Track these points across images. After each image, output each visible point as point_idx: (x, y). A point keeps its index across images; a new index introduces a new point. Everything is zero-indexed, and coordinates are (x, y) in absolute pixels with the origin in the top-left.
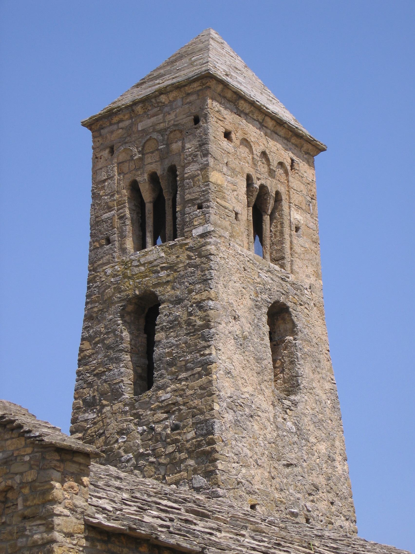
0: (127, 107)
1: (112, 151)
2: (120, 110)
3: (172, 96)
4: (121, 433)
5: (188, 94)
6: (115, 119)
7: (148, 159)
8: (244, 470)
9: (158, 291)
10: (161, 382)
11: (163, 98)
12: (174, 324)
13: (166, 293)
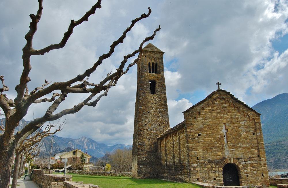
0: (150, 51)
1: (146, 56)
2: (148, 51)
4: (151, 99)
6: (147, 52)
7: (152, 60)
10: (157, 94)
11: (156, 53)
12: (159, 86)
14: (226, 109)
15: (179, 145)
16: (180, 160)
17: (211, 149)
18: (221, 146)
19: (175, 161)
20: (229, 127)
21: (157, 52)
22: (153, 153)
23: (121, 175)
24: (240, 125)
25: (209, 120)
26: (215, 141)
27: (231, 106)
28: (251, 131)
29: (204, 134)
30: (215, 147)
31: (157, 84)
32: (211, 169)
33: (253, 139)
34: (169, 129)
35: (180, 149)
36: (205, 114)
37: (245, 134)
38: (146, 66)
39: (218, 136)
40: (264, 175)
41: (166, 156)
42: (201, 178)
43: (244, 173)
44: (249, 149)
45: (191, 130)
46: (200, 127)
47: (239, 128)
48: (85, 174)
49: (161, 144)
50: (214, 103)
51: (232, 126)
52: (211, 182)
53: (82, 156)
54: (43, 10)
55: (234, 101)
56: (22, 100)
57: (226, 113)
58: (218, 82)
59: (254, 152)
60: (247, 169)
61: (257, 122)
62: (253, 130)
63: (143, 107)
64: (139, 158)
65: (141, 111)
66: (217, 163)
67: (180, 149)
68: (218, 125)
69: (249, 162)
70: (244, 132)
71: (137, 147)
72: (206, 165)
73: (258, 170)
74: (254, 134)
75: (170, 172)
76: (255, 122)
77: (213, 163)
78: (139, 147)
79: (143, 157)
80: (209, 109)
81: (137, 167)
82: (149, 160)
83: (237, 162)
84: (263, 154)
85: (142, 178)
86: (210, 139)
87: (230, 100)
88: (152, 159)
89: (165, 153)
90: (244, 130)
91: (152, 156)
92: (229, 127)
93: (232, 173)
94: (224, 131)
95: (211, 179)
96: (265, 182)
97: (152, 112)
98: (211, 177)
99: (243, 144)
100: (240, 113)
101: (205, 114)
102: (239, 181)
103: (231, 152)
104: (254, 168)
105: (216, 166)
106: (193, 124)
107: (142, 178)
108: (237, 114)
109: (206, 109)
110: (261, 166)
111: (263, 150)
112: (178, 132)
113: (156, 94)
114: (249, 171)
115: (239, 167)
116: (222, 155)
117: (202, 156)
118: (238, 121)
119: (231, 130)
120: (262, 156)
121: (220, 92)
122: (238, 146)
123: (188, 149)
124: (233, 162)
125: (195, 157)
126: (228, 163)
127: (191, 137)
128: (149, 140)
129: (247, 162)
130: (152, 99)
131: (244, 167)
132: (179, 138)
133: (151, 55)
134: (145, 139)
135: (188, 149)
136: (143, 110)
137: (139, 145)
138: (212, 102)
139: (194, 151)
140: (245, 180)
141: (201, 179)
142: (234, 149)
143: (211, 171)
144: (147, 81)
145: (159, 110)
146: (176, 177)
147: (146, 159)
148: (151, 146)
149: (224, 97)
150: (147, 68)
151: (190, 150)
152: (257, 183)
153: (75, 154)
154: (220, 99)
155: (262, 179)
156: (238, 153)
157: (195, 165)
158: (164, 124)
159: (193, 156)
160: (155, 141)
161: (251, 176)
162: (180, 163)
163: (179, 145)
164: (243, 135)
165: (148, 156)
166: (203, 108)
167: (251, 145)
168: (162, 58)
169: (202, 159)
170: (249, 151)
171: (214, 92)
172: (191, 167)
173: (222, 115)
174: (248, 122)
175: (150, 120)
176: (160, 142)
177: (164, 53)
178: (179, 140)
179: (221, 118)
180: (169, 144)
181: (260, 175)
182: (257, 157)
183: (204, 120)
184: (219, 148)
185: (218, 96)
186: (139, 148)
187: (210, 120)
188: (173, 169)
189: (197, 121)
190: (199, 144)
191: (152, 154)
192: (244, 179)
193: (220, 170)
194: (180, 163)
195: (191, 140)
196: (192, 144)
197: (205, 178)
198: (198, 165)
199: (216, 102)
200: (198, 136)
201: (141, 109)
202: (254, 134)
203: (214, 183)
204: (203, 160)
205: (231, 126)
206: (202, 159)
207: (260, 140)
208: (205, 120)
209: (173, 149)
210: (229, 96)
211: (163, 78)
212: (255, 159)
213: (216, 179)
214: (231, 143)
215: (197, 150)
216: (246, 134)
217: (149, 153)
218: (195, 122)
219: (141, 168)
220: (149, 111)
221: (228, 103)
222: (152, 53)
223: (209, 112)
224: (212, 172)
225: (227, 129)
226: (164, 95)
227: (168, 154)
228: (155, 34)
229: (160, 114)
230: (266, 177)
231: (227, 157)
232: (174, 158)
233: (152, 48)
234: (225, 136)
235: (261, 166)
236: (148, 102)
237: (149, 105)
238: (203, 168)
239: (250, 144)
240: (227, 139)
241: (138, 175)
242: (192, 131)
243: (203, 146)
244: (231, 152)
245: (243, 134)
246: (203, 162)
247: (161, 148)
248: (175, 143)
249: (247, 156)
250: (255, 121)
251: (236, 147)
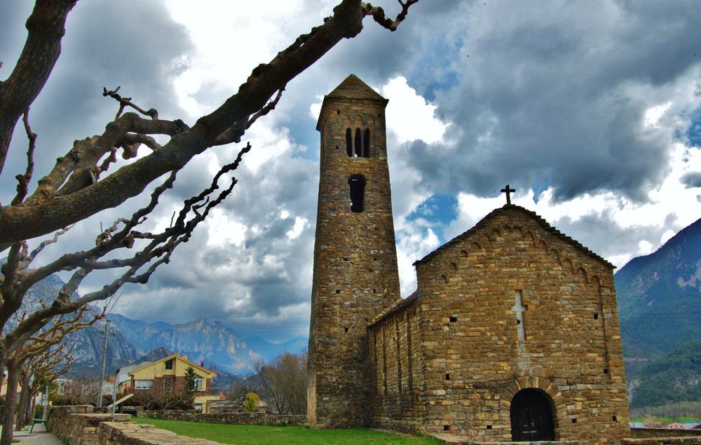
0: (349, 98)
1: (339, 113)
2: (345, 98)
3: (369, 102)
5: (376, 105)
6: (342, 101)
7: (357, 122)
9: (366, 175)
10: (369, 210)
11: (366, 102)
12: (372, 190)
14: (523, 253)
15: (409, 344)
16: (410, 381)
17: (483, 354)
18: (509, 346)
19: (402, 383)
20: (530, 299)
21: (368, 99)
22: (356, 365)
23: (287, 422)
24: (561, 294)
26: (494, 333)
27: (537, 245)
28: (587, 309)
29: (465, 316)
30: (494, 350)
31: (369, 185)
32: (480, 403)
33: (594, 328)
34: (398, 301)
35: (410, 355)
36: (470, 267)
37: (572, 316)
38: (341, 138)
39: (501, 322)
40: (618, 418)
41: (385, 372)
42: (454, 424)
44: (581, 352)
45: (433, 307)
46: (456, 299)
47: (558, 303)
48: (192, 418)
49: (375, 340)
50: (495, 240)
51: (538, 297)
52: (480, 434)
53: (190, 371)
54: (34, 167)
55: (546, 233)
56: (12, 286)
58: (507, 187)
59: (594, 360)
60: (573, 404)
61: (605, 287)
62: (596, 305)
63: (330, 247)
64: (320, 377)
65: (325, 256)
66: (495, 388)
67: (410, 355)
68: (503, 294)
69: (580, 386)
70: (571, 313)
71: (315, 349)
72: (468, 393)
73: (601, 406)
74: (596, 317)
75: (391, 412)
76: (600, 287)
77: (486, 388)
78: (320, 348)
79: (331, 375)
80: (481, 254)
81: (315, 400)
82: (346, 381)
83: (547, 387)
84: (617, 367)
85: (327, 428)
86: (482, 329)
87: (537, 232)
88: (354, 378)
89: (383, 363)
90: (570, 306)
91: (355, 371)
92: (530, 299)
93: (533, 410)
94: (517, 310)
95: (480, 427)
96: (619, 436)
97: (354, 258)
98: (480, 422)
99: (565, 342)
100: (560, 264)
101: (470, 267)
102: (553, 432)
103: (535, 360)
104: (592, 400)
105: (493, 396)
106: (438, 293)
107: (327, 428)
108: (555, 267)
109: (472, 256)
110: (612, 397)
111: (617, 356)
112: (406, 312)
113: (366, 210)
114: (579, 406)
115: (553, 398)
116: (509, 368)
117: (457, 372)
118: (554, 285)
119: (537, 306)
120: (616, 370)
122: (553, 346)
123: (424, 355)
124: (537, 387)
125: (440, 375)
126: (524, 388)
127: (431, 324)
128: (346, 330)
129: (574, 386)
130: (355, 226)
131: (567, 399)
132: (409, 327)
133: (354, 108)
134: (336, 329)
135: (424, 355)
136: (331, 254)
137: (321, 344)
138: (489, 237)
139: (439, 360)
140: (568, 431)
141: (454, 428)
142: (542, 355)
143: (480, 408)
144: (342, 177)
145: (372, 252)
146: (403, 422)
147: (337, 380)
148: (350, 345)
150: (342, 142)
151: (428, 356)
152: (600, 437)
153: (171, 368)
154: (510, 228)
155: (611, 427)
156: (551, 363)
157: (441, 392)
158: (386, 290)
159: (437, 372)
160: (363, 332)
161: (584, 419)
162: (411, 389)
163: (409, 344)
164: (566, 319)
165: (344, 372)
166: (465, 253)
167: (588, 345)
168: (382, 117)
169: (459, 378)
170: (581, 360)
171: (495, 211)
172: (429, 398)
173: (512, 270)
174: (583, 285)
175: (348, 278)
176: (375, 336)
177: (386, 101)
178: (409, 332)
179: (511, 277)
180: (391, 340)
181: (609, 418)
182: (603, 374)
183: (465, 284)
184: (503, 351)
185: (504, 222)
186: (321, 353)
187: (482, 282)
188: (398, 403)
189: (450, 286)
190: (451, 341)
191: (354, 367)
192: (565, 426)
193: (504, 405)
194: (411, 389)
195: (432, 333)
196: (433, 343)
197: (464, 424)
198: (447, 394)
199: (500, 236)
200: (451, 323)
201: (325, 250)
202: (596, 317)
203: (487, 437)
204: (462, 382)
205: (535, 298)
206: (458, 379)
207: (611, 332)
208: (470, 281)
209: (399, 353)
210: (532, 221)
211: (384, 168)
212: (596, 378)
213: (493, 427)
214: (536, 339)
215: (447, 356)
217: (349, 363)
218: (442, 289)
219: (327, 402)
220: (345, 257)
221: (531, 239)
222: (357, 103)
223: (480, 263)
224: (482, 411)
225: (526, 304)
226: (387, 212)
227: (390, 367)
228: (239, 159)
229: (377, 263)
230: (623, 422)
231: (522, 374)
232: (400, 375)
233: (357, 89)
234: (521, 321)
235: (612, 395)
236: (343, 233)
237: (347, 240)
238: (460, 401)
239: (584, 341)
240: (525, 329)
241: (318, 420)
242: (433, 309)
243: (463, 347)
244: (535, 360)
246: (462, 385)
247: (375, 351)
248: (402, 338)
249: (575, 371)
250: (599, 284)
251: (548, 349)
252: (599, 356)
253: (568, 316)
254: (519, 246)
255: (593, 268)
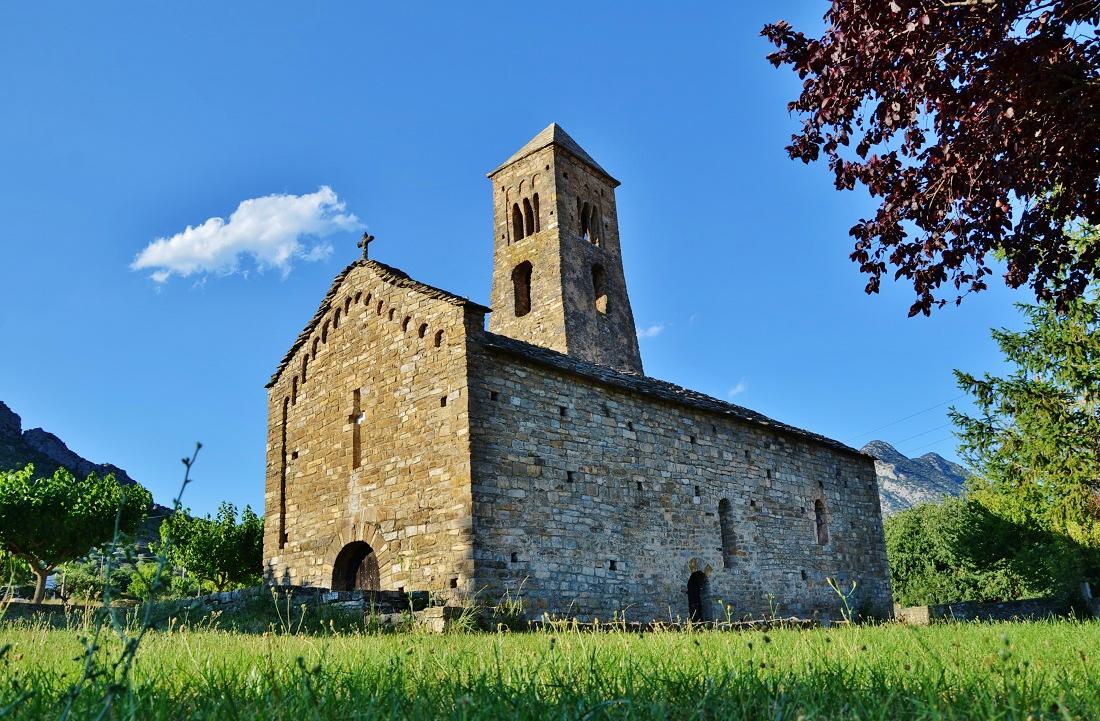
1: (503, 189)
8: (582, 352)
11: (529, 158)
13: (534, 262)
14: (364, 331)
25: (321, 394)
26: (329, 465)
28: (433, 392)
33: (440, 424)
43: (389, 578)
47: (396, 395)
51: (377, 393)
57: (364, 348)
62: (445, 381)
69: (411, 530)
70: (412, 406)
86: (318, 461)
103: (367, 496)
113: (532, 308)
121: (352, 273)
124: (361, 540)
149: (358, 288)
164: (405, 419)
170: (421, 484)
173: (351, 362)
179: (351, 374)
183: (308, 401)
187: (323, 393)
212: (439, 512)
216: (416, 409)
245: (406, 414)
252: (445, 472)
253: (409, 412)
254: (359, 323)
255: (439, 318)
